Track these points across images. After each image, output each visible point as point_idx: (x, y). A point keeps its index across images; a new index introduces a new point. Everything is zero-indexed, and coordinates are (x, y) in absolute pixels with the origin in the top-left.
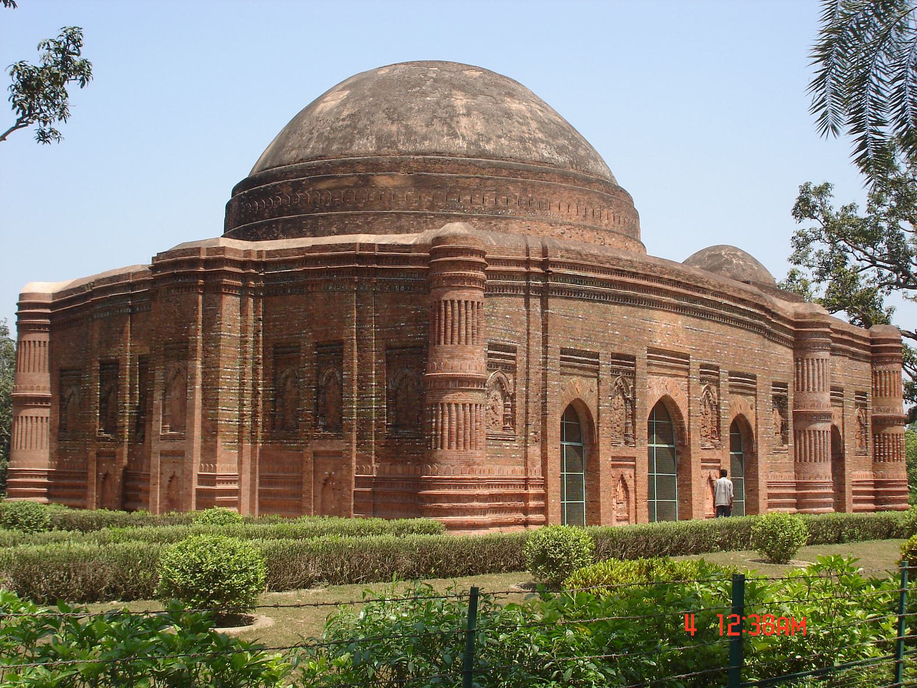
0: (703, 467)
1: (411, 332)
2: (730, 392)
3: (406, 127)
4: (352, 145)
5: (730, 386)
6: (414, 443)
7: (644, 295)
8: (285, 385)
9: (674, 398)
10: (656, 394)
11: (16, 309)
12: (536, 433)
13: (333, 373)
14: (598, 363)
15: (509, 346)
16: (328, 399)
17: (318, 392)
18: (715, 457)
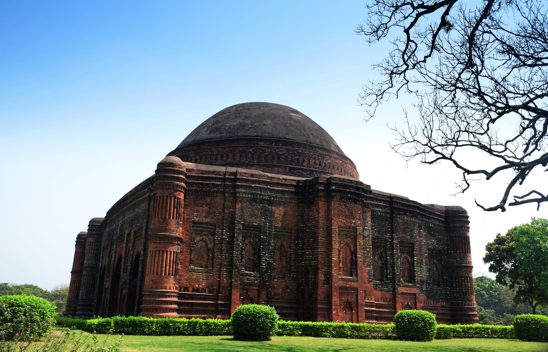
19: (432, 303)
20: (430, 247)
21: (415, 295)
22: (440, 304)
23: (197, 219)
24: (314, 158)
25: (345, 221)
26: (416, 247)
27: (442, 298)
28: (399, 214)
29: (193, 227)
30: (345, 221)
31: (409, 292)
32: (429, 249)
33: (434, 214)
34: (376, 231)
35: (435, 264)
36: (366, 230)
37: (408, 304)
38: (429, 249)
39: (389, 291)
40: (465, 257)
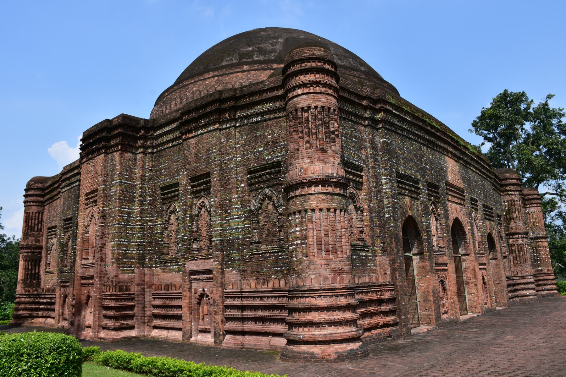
0: (480, 269)
1: (269, 154)
2: (486, 218)
3: (259, 48)
4: (222, 61)
5: (484, 214)
6: (277, 257)
7: (439, 143)
8: (169, 219)
9: (461, 220)
10: (453, 215)
11: (24, 193)
12: (384, 243)
13: (203, 202)
14: (419, 188)
15: (358, 166)
16: (200, 225)
17: (192, 219)
18: (484, 262)
19: (253, 284)
20: (253, 165)
21: (209, 272)
22: (270, 285)
23: (49, 225)
24: (175, 99)
25: (89, 185)
26: (215, 179)
27: (277, 272)
28: (190, 131)
29: (49, 232)
30: (89, 185)
31: (201, 268)
32: (250, 172)
33: (261, 92)
34: (165, 176)
35: (270, 199)
36: (113, 186)
37: (204, 290)
38: (250, 172)
39: (179, 270)
40: (291, 164)
